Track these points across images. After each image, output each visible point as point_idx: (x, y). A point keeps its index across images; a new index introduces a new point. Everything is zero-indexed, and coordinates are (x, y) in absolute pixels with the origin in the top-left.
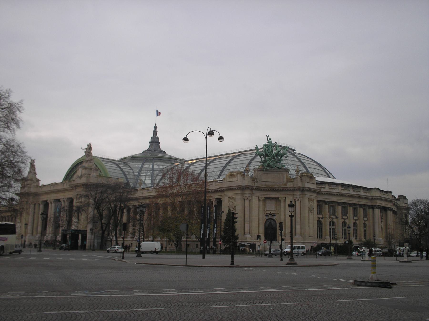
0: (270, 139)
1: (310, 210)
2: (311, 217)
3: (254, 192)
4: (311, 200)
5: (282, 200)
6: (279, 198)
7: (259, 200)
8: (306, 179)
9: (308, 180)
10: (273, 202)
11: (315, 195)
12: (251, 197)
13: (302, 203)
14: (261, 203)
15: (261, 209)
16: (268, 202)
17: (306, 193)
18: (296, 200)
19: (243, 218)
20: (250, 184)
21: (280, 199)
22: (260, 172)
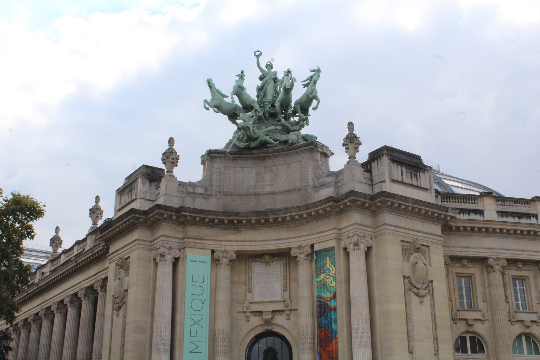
0: (269, 66)
1: (417, 287)
2: (421, 312)
3: (193, 231)
4: (417, 250)
5: (302, 257)
6: (290, 249)
7: (215, 261)
8: (385, 165)
9: (397, 172)
10: (277, 268)
11: (437, 229)
12: (178, 254)
13: (374, 260)
14: (224, 272)
15: (223, 296)
16: (258, 269)
17: (388, 218)
18: (351, 247)
19: (148, 332)
20: (175, 203)
21: (293, 253)
22: (218, 165)
